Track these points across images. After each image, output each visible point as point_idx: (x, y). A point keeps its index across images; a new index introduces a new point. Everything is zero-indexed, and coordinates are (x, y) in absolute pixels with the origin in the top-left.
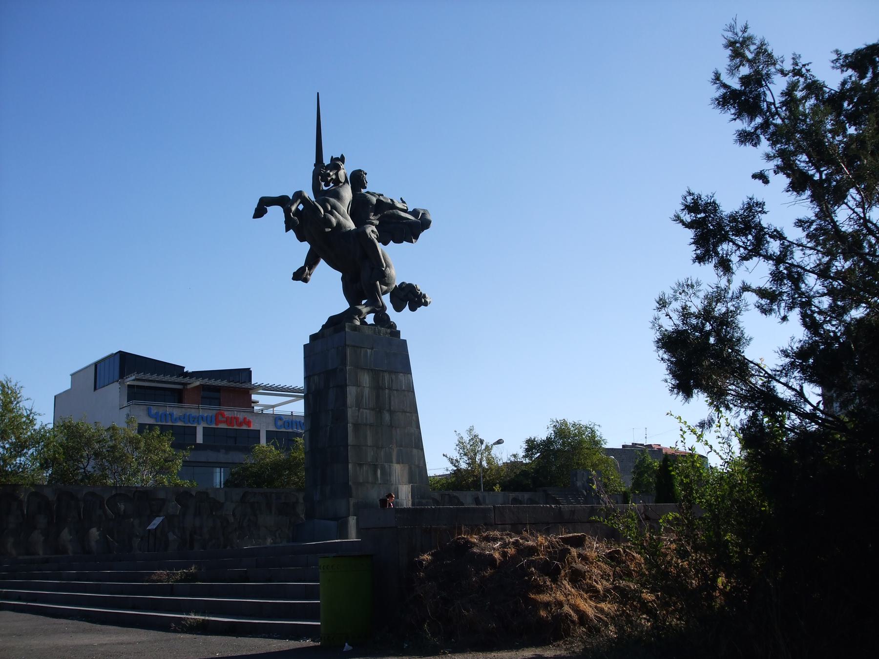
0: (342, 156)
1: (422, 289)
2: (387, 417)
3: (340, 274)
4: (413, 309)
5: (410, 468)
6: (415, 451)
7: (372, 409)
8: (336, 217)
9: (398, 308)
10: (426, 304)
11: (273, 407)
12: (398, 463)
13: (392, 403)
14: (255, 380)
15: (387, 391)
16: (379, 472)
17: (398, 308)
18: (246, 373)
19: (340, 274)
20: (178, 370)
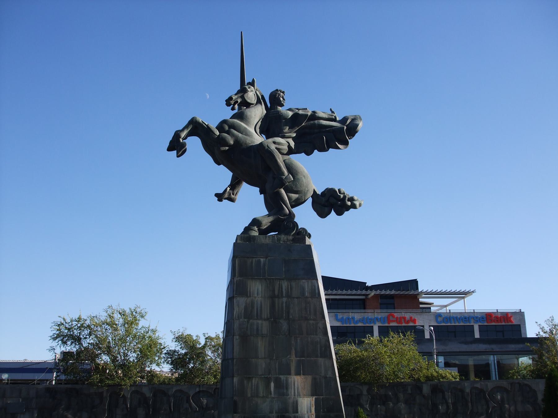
0: (253, 80)
1: (349, 192)
2: (284, 326)
3: (258, 189)
4: (340, 213)
5: (314, 380)
6: (321, 361)
7: (267, 319)
8: (233, 135)
9: (323, 214)
10: (354, 206)
11: (446, 306)
12: (298, 373)
13: (291, 311)
14: (422, 287)
15: (285, 300)
16: (272, 385)
17: (323, 214)
18: (414, 283)
19: (258, 189)
20: (361, 285)
